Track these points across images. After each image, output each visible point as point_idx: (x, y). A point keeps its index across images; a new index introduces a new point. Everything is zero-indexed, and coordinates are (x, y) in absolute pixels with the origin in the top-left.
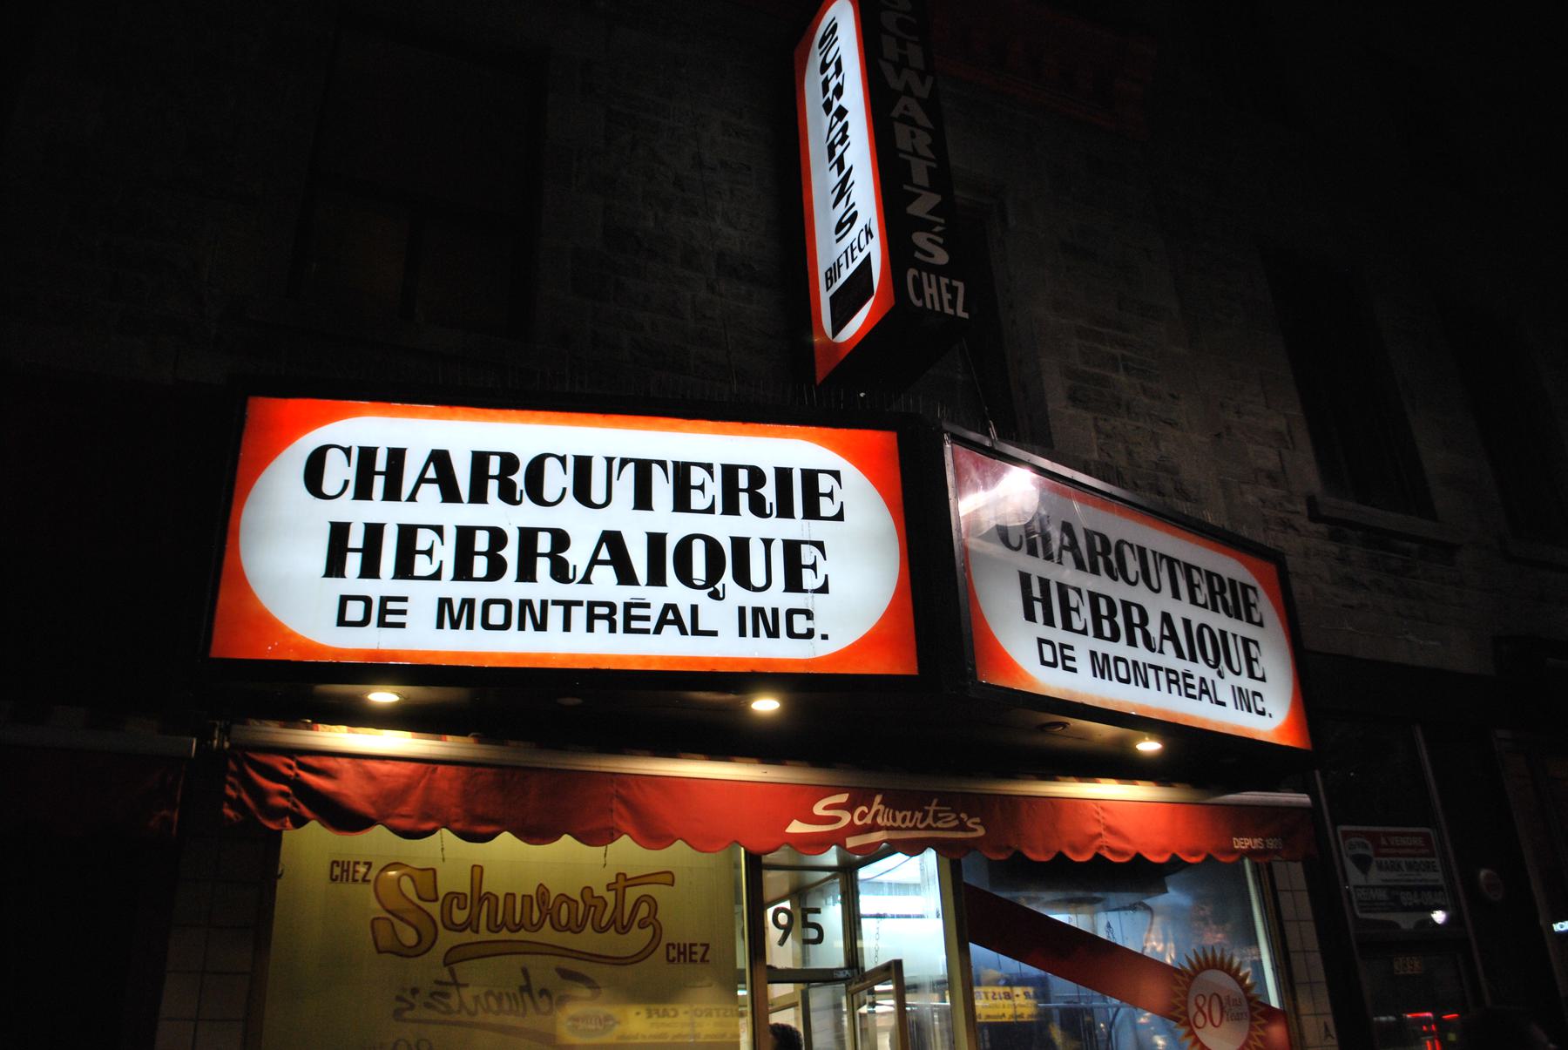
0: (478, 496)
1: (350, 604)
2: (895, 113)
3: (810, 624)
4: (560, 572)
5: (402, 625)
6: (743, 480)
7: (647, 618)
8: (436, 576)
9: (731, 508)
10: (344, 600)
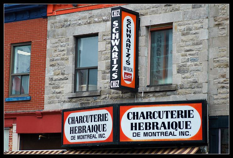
3: (188, 133)
4: (157, 128)
7: (168, 134)
8: (143, 129)
10: (133, 133)
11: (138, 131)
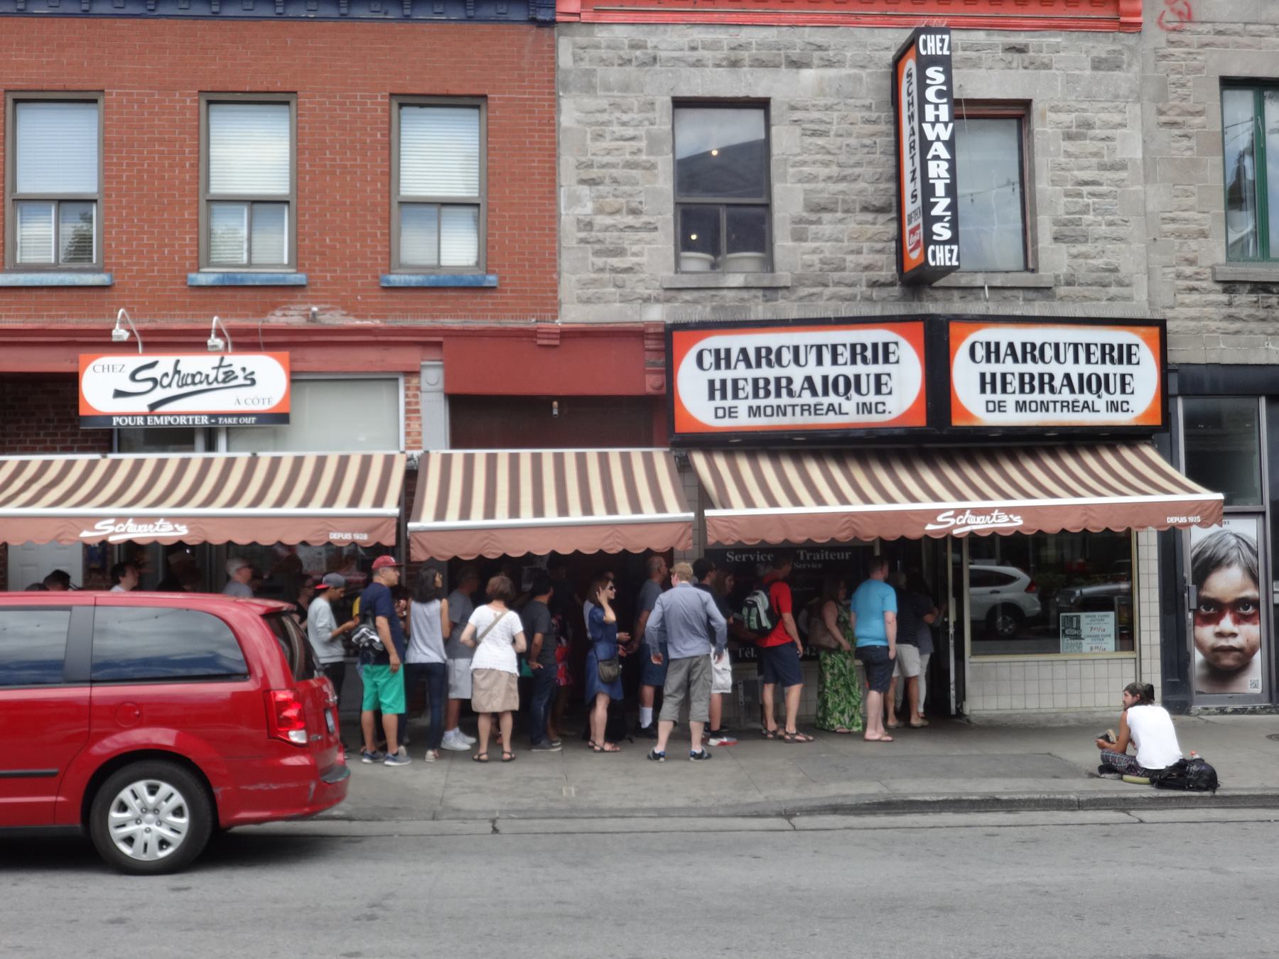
2: (929, 156)
5: (736, 417)
6: (859, 349)
7: (822, 409)
8: (747, 398)
10: (716, 409)
11: (729, 402)
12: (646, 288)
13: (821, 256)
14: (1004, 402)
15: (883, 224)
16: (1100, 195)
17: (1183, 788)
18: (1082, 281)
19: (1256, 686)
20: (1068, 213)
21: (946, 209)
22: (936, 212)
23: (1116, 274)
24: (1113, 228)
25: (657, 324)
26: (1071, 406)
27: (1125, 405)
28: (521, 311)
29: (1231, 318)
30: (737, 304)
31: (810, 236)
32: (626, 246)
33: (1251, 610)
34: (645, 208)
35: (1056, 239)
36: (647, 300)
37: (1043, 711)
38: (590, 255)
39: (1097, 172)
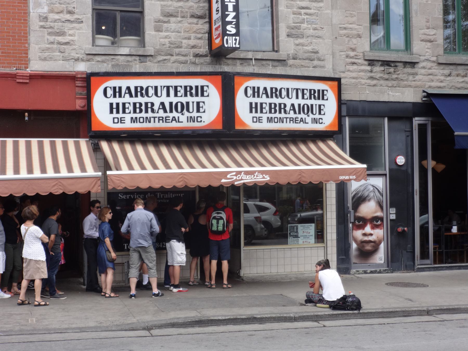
0: (136, 96)
1: (115, 119)
4: (153, 111)
5: (124, 123)
7: (169, 120)
8: (130, 113)
9: (186, 95)
10: (114, 118)
12: (77, 54)
13: (169, 40)
14: (262, 117)
15: (202, 24)
16: (310, 15)
17: (344, 309)
18: (300, 57)
19: (381, 260)
20: (294, 23)
21: (233, 18)
22: (229, 19)
23: (317, 55)
24: (316, 31)
25: (82, 73)
26: (294, 120)
27: (320, 120)
28: (8, 63)
29: (372, 78)
30: (126, 63)
31: (164, 29)
32: (66, 30)
33: (379, 223)
34: (76, 11)
35: (288, 35)
36: (77, 60)
37: (279, 274)
38: (46, 34)
39: (308, 3)
